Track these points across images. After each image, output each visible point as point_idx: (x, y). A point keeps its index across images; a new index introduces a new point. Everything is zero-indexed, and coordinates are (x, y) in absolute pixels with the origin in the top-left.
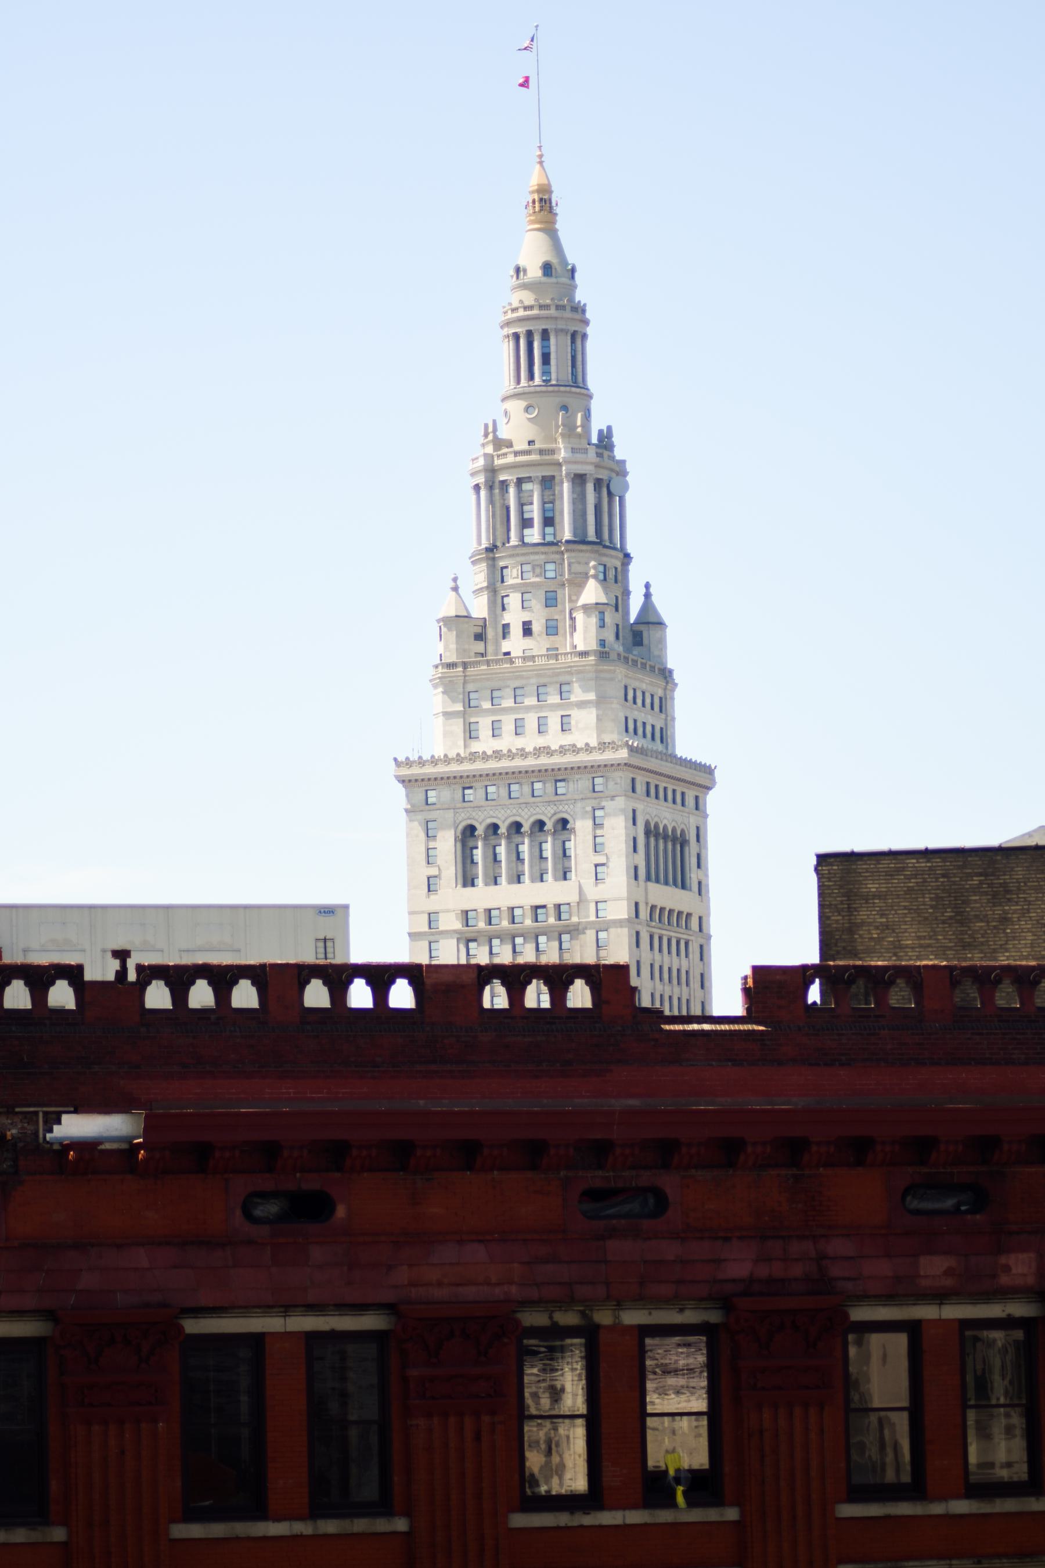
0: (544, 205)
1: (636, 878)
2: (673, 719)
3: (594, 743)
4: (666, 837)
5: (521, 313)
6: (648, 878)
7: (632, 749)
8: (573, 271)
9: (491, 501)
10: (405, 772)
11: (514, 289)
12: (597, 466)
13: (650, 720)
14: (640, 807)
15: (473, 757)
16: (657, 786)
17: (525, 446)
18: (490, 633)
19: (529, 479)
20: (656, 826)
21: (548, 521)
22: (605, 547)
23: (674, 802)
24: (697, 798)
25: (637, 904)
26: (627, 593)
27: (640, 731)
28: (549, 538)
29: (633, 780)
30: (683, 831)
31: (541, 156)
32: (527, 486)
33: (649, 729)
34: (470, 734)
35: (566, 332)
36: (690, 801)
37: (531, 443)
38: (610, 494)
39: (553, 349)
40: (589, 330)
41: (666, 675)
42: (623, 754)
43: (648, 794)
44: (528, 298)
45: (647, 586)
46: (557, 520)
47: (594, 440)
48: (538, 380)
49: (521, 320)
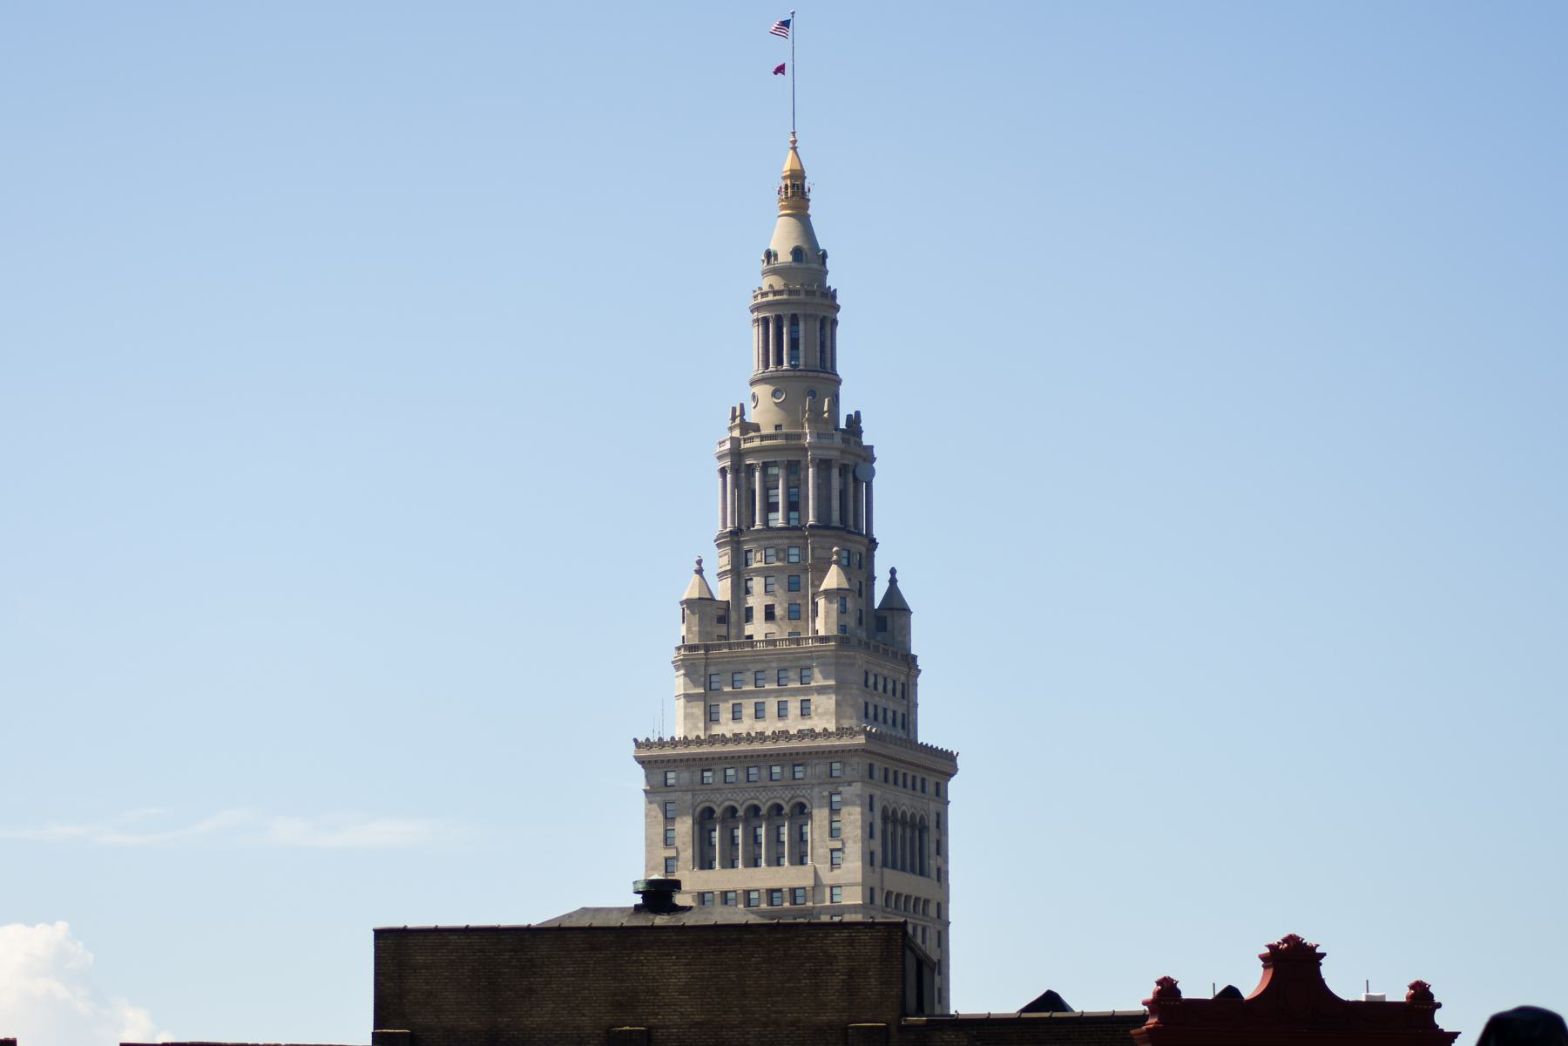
0: (796, 194)
1: (872, 864)
2: (916, 705)
3: (832, 728)
4: (904, 823)
5: (771, 297)
6: (884, 864)
7: (869, 735)
8: (824, 256)
9: (736, 485)
10: (644, 753)
11: (764, 273)
12: (843, 452)
13: (891, 706)
14: (877, 793)
15: (713, 740)
16: (896, 773)
17: (771, 431)
18: (733, 617)
19: (775, 464)
20: (894, 812)
21: (793, 505)
22: (850, 532)
23: (914, 788)
24: (938, 784)
25: (872, 890)
26: (871, 579)
27: (881, 717)
28: (794, 523)
29: (871, 766)
30: (922, 818)
31: (794, 142)
32: (773, 471)
33: (890, 714)
34: (711, 717)
35: (815, 317)
36: (931, 788)
37: (778, 427)
38: (856, 480)
39: (801, 334)
40: (839, 316)
41: (910, 662)
42: (861, 739)
43: (886, 780)
44: (778, 283)
45: (893, 572)
46: (802, 504)
47: (843, 425)
48: (786, 365)
49: (769, 305)
